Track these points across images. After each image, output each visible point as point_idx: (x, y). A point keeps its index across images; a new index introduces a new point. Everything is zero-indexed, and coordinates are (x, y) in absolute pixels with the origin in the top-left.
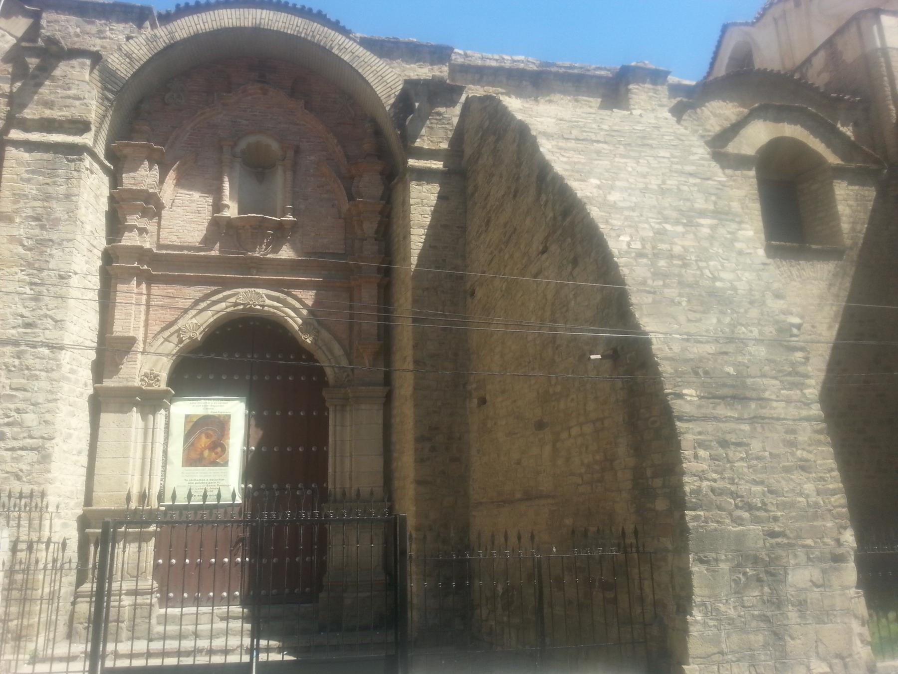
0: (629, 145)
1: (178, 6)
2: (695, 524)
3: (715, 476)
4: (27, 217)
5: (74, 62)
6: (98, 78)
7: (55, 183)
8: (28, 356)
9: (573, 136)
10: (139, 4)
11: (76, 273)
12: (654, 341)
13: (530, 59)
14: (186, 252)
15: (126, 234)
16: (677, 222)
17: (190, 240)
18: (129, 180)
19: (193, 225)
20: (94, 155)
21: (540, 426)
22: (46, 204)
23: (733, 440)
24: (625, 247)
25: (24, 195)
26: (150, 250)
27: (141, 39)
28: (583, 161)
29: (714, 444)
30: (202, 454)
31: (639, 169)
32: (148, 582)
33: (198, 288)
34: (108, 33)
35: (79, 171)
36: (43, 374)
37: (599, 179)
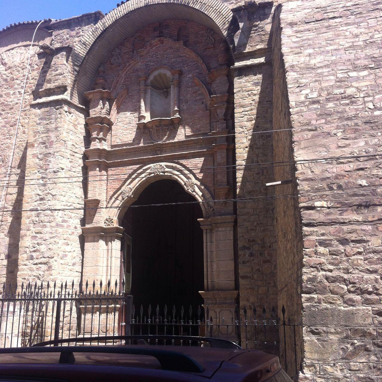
2: (308, 304)
3: (331, 267)
5: (59, 55)
6: (71, 60)
8: (42, 215)
11: (63, 169)
12: (299, 167)
14: (125, 147)
15: (93, 143)
16: (366, 68)
17: (126, 140)
18: (94, 113)
19: (127, 131)
22: (47, 135)
23: (353, 239)
24: (302, 98)
25: (38, 132)
29: (335, 243)
33: (131, 167)
36: (48, 224)
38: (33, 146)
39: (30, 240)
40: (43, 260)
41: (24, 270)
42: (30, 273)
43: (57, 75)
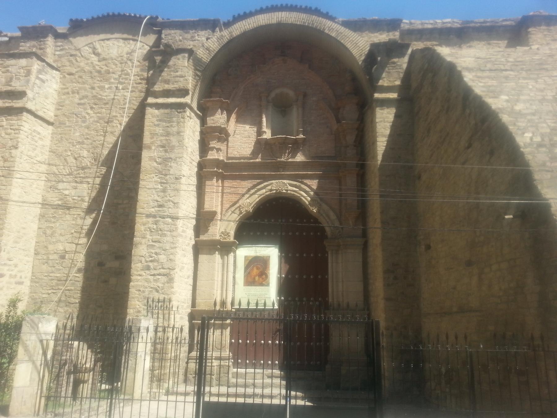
0: (530, 70)
1: (234, 16)
4: (158, 146)
5: (180, 56)
6: (192, 64)
7: (171, 126)
8: (160, 223)
9: (487, 68)
10: (212, 18)
11: (184, 176)
12: (553, 205)
13: (455, 20)
14: (242, 161)
15: (210, 152)
17: (245, 153)
18: (211, 121)
19: (246, 145)
20: (191, 109)
21: (469, 263)
22: (167, 138)
24: (528, 140)
26: (223, 161)
27: (215, 39)
28: (495, 84)
30: (254, 279)
31: (537, 86)
32: (226, 353)
33: (250, 181)
34: (197, 38)
35: (183, 118)
36: (169, 233)
37: (508, 95)
38: (149, 148)
39: (145, 249)
40: (162, 271)
41: (138, 281)
42: (146, 284)
43: (177, 77)
